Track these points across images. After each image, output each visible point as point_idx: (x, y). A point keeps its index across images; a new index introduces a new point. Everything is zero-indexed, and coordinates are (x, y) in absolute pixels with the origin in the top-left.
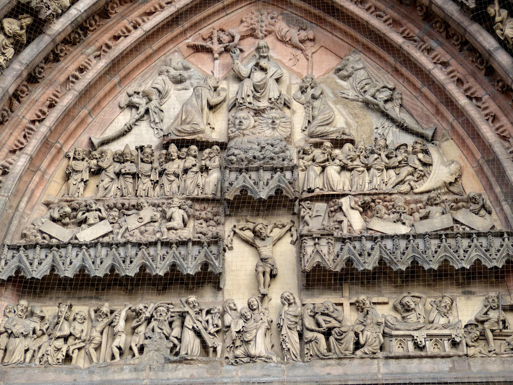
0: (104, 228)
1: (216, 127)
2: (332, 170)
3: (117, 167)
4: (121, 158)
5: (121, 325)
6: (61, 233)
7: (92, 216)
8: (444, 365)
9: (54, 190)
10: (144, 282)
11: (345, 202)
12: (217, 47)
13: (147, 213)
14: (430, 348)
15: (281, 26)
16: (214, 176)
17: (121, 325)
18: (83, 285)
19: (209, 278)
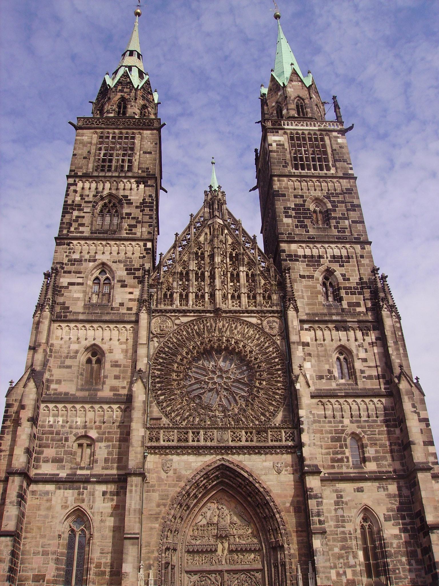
0: (200, 541)
1: (215, 520)
2: (234, 530)
3: (201, 528)
4: (201, 526)
5: (204, 559)
6: (193, 542)
7: (198, 539)
8: (249, 566)
9: (191, 533)
10: (207, 552)
11: (236, 536)
12: (215, 502)
13: (206, 539)
14: (247, 563)
15: (226, 498)
16: (216, 531)
17: (204, 559)
18: (198, 552)
19: (216, 550)
